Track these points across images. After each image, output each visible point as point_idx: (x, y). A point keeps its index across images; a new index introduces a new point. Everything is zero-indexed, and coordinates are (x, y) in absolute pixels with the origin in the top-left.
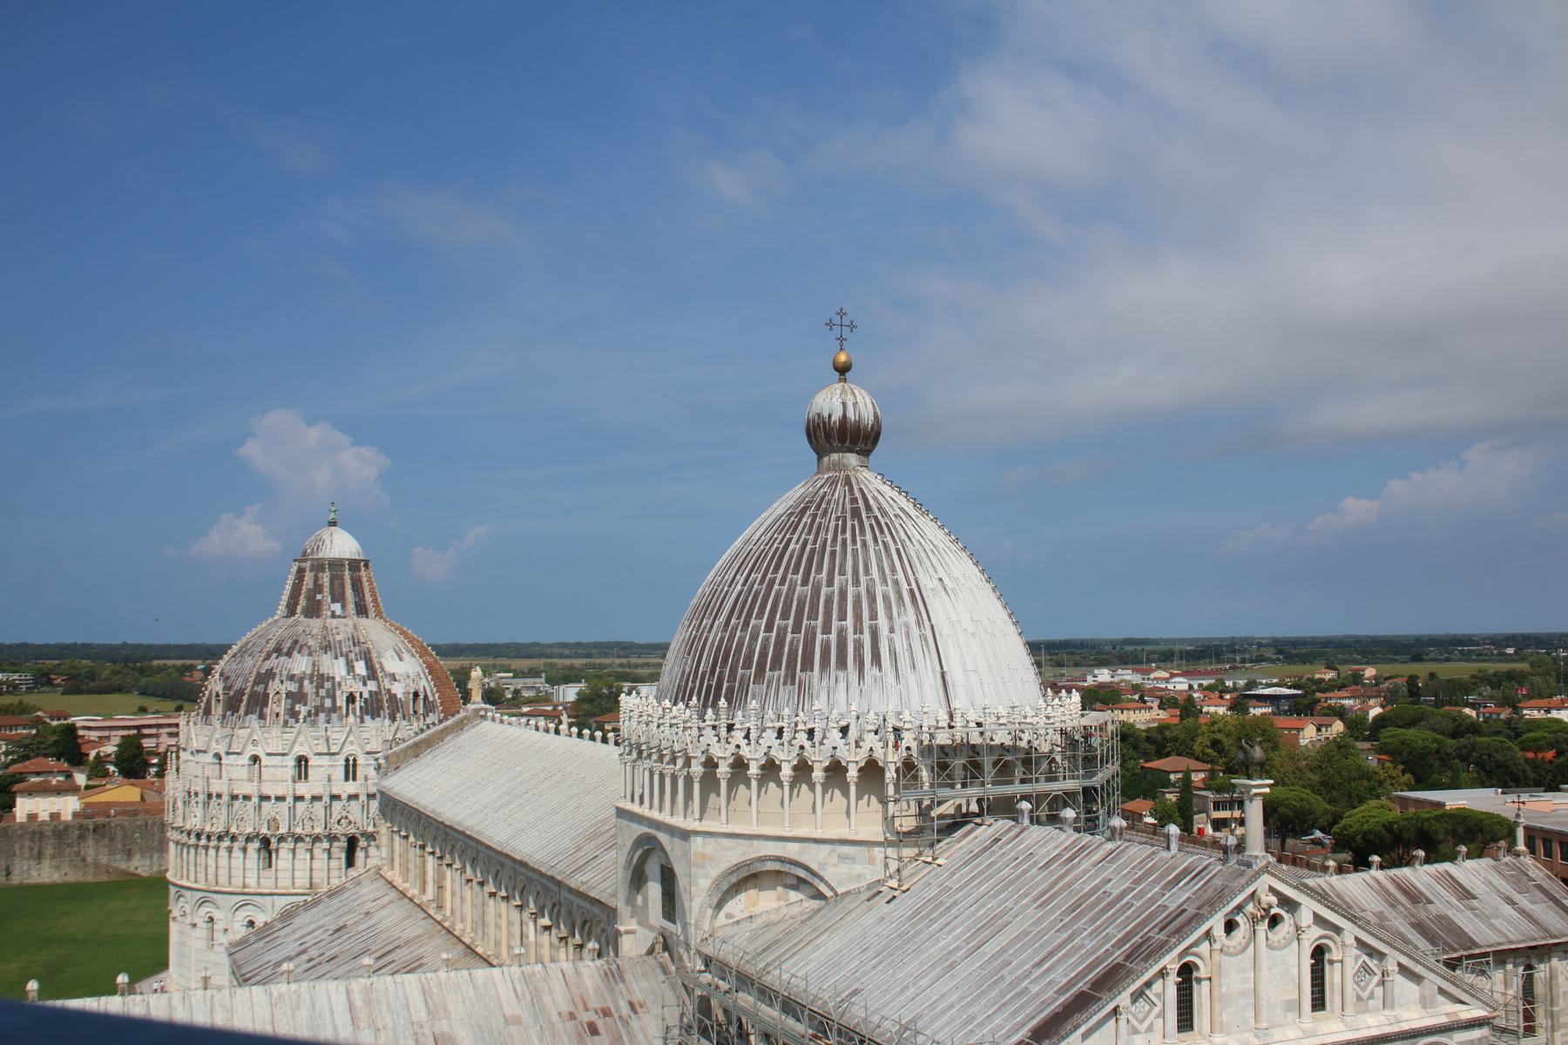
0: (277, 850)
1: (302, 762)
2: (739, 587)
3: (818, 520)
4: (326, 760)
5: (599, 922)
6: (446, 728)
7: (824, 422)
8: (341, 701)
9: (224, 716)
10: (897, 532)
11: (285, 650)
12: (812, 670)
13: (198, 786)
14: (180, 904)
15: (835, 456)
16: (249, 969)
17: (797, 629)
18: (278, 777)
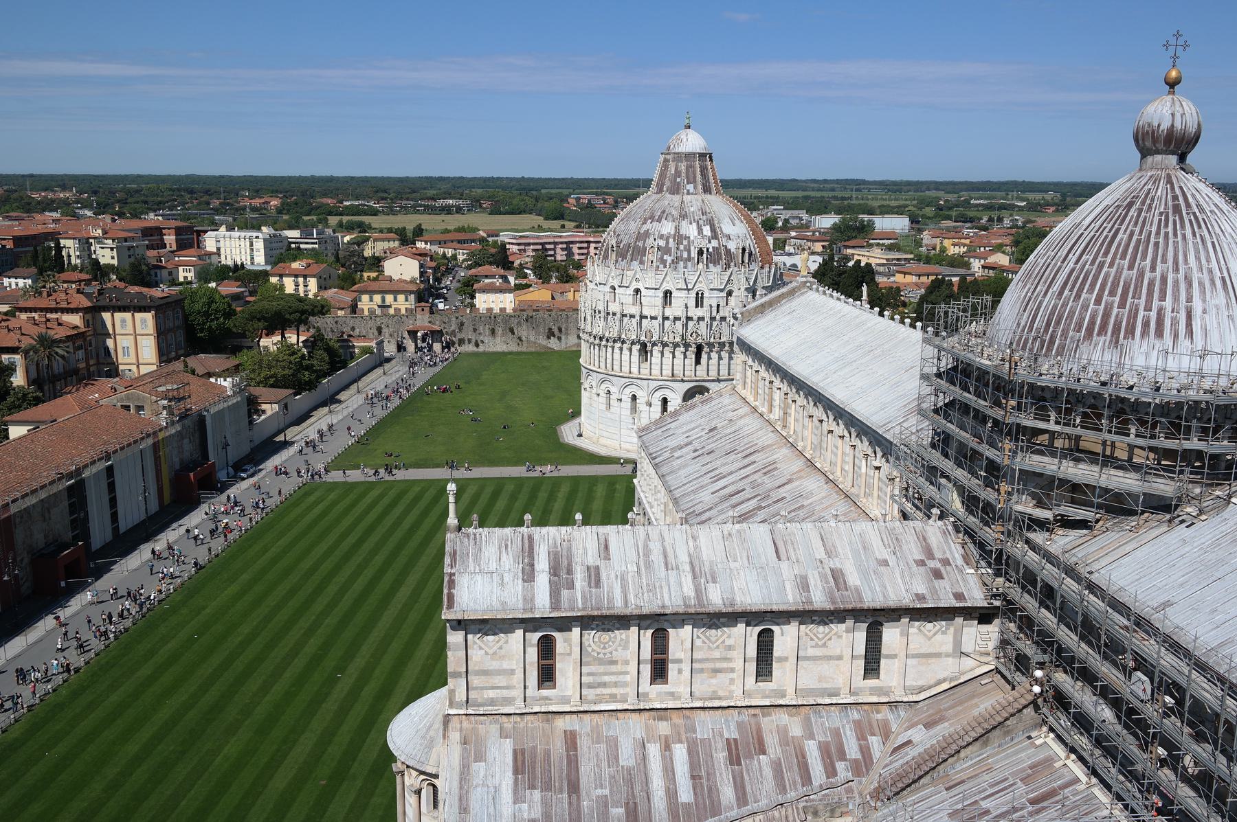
0: (651, 351)
1: (668, 295)
2: (1071, 265)
3: (1143, 214)
7: (1153, 132)
8: (694, 254)
9: (617, 261)
12: (1133, 339)
13: (601, 307)
14: (589, 380)
15: (1158, 158)
16: (654, 450)
17: (1122, 305)
18: (653, 302)
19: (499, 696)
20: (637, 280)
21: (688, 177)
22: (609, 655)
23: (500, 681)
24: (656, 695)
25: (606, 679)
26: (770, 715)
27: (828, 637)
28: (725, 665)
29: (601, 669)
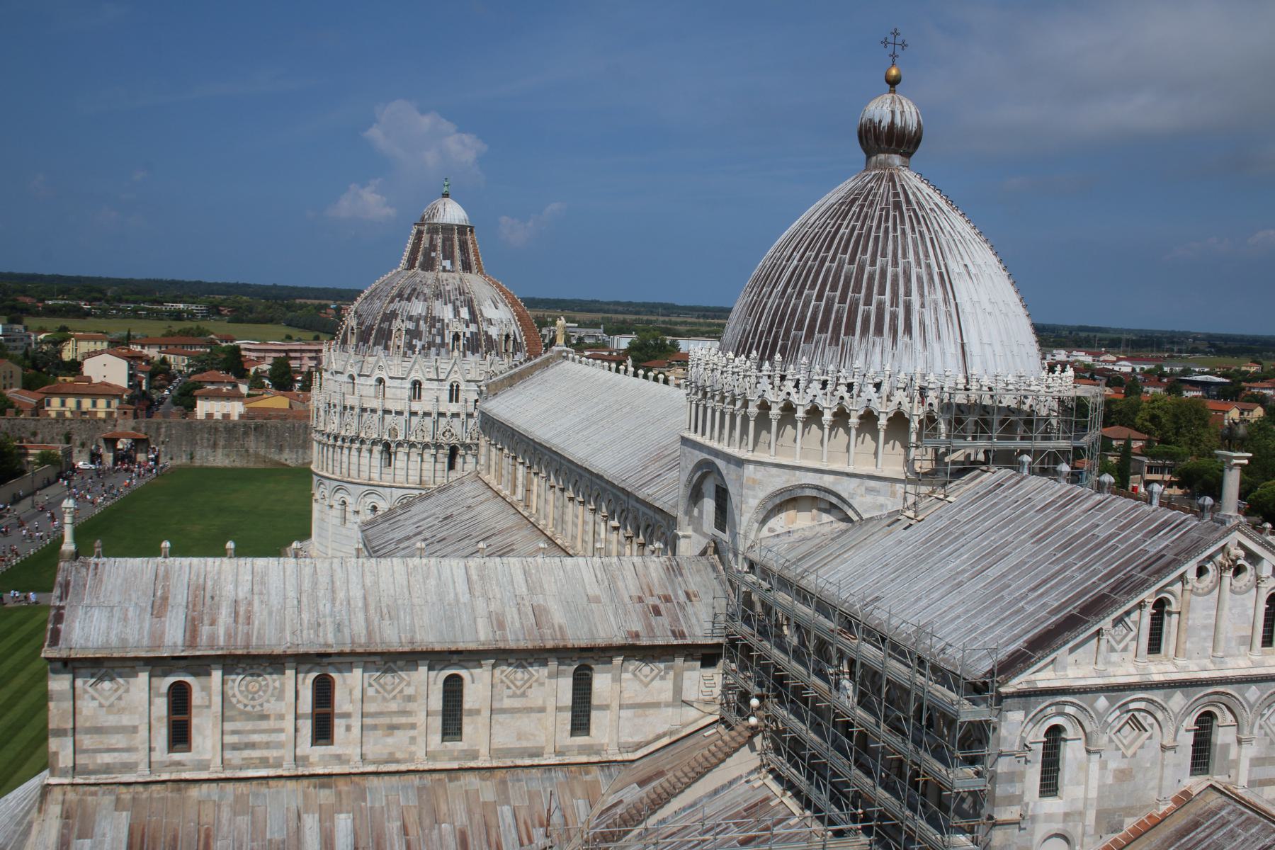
0: (396, 453)
1: (417, 385)
2: (795, 262)
3: (865, 210)
4: (435, 385)
5: (661, 526)
6: (535, 365)
7: (875, 127)
8: (449, 339)
10: (932, 223)
11: (406, 296)
12: (854, 335)
13: (336, 400)
14: (321, 490)
15: (882, 157)
17: (843, 300)
18: (398, 395)
19: (117, 760)
20: (380, 368)
21: (444, 251)
22: (258, 708)
23: (118, 741)
24: (319, 758)
25: (256, 738)
26: (457, 779)
27: (527, 685)
28: (403, 720)
29: (249, 726)
